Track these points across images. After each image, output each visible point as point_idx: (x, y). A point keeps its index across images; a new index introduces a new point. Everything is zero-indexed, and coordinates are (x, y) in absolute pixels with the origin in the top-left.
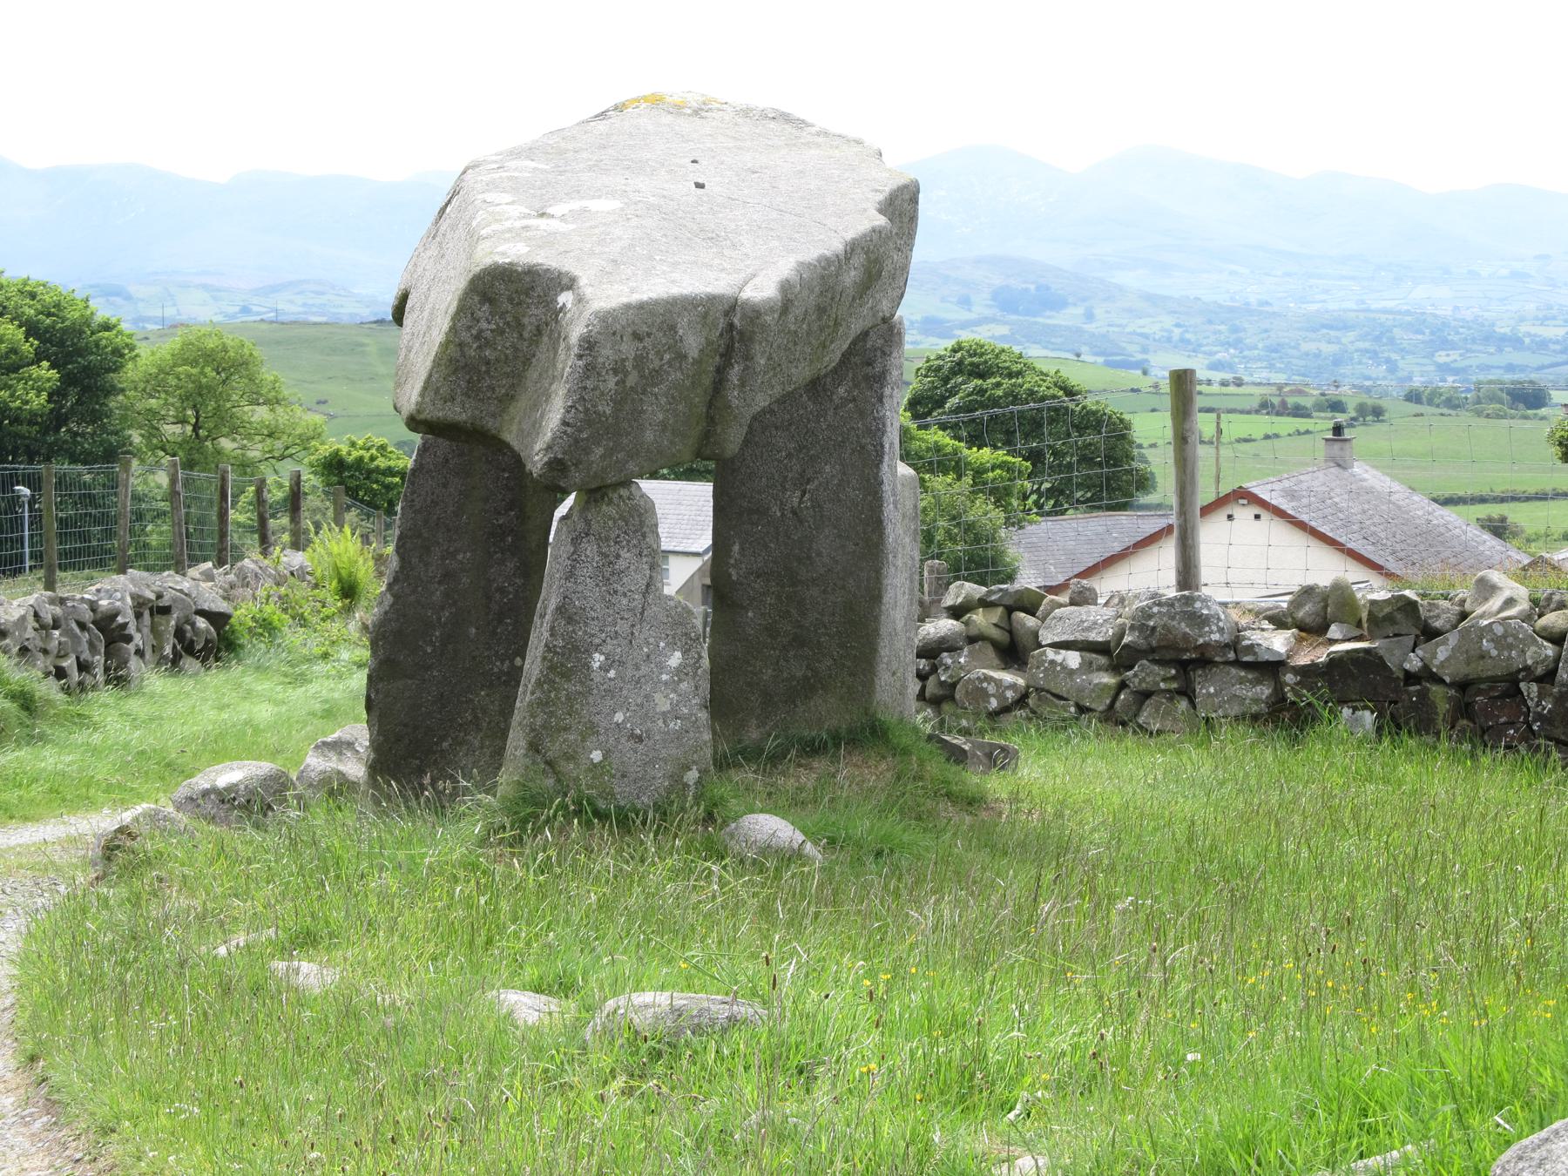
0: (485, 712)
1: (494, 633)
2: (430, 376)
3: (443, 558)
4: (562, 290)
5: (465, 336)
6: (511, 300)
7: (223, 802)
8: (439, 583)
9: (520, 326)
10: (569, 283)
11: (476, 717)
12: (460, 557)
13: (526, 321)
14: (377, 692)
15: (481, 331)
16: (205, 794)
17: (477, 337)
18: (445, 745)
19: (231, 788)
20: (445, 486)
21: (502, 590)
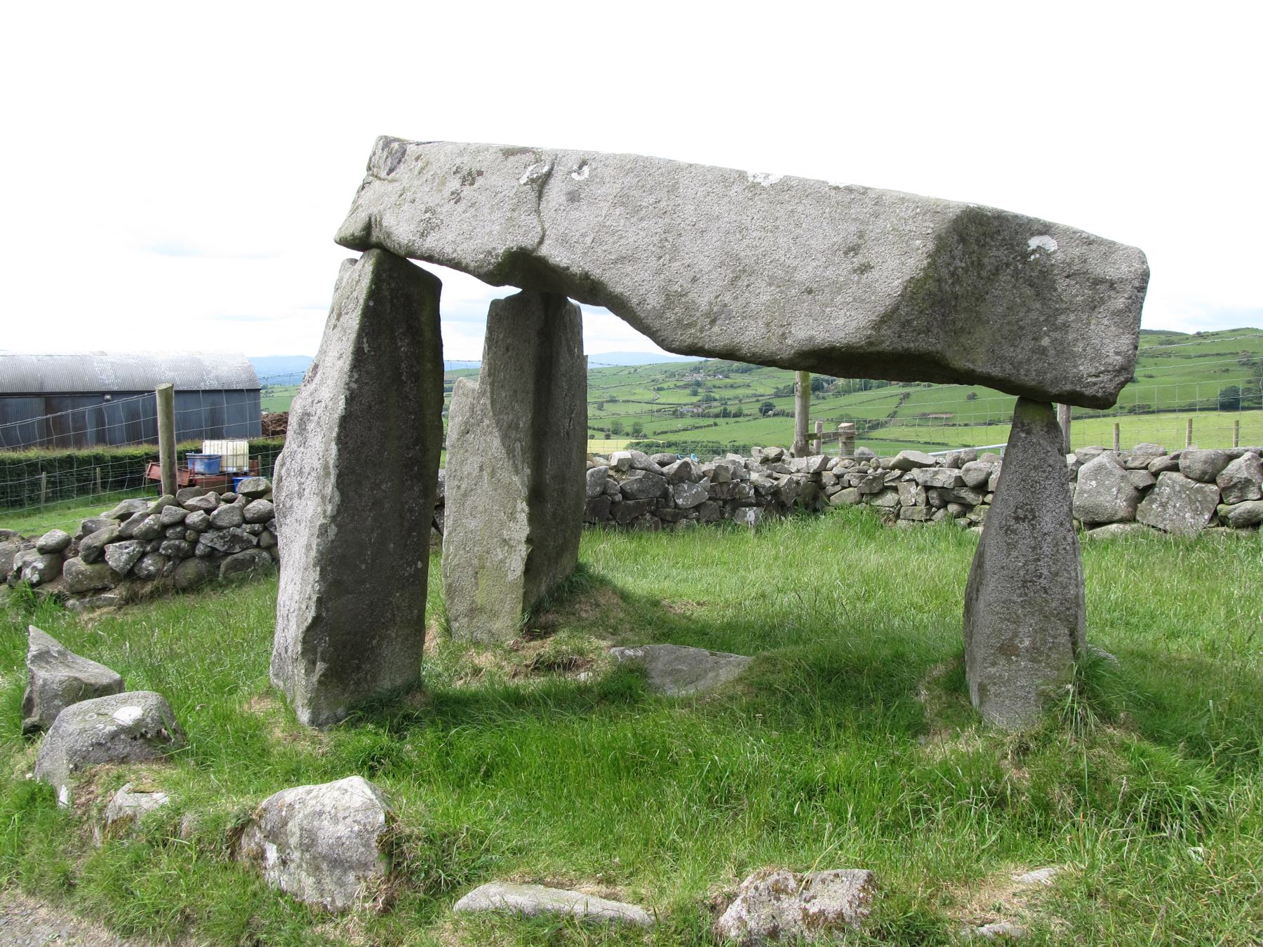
0: (399, 608)
1: (406, 545)
2: (896, 309)
3: (372, 489)
4: (1032, 235)
5: (944, 272)
6: (978, 241)
7: (135, 738)
8: (370, 510)
9: (981, 265)
10: (1046, 229)
11: (394, 615)
12: (383, 487)
13: (986, 261)
14: (327, 610)
15: (956, 268)
16: (114, 736)
17: (953, 274)
18: (374, 642)
19: (139, 723)
20: (370, 429)
21: (411, 510)
